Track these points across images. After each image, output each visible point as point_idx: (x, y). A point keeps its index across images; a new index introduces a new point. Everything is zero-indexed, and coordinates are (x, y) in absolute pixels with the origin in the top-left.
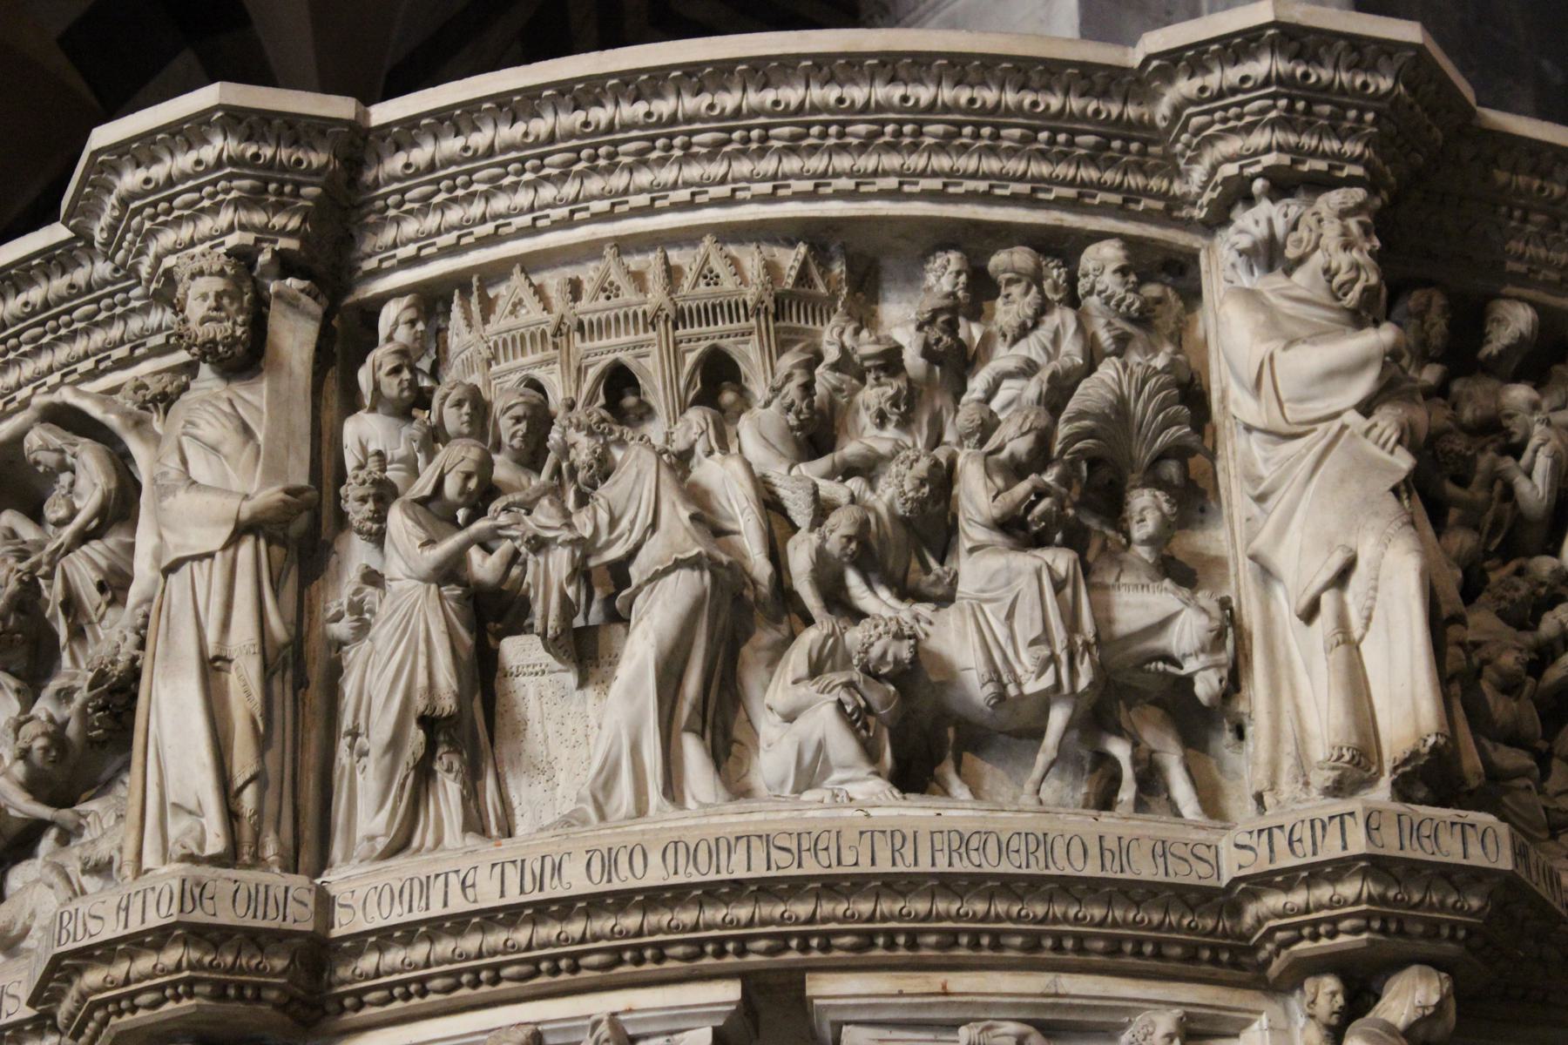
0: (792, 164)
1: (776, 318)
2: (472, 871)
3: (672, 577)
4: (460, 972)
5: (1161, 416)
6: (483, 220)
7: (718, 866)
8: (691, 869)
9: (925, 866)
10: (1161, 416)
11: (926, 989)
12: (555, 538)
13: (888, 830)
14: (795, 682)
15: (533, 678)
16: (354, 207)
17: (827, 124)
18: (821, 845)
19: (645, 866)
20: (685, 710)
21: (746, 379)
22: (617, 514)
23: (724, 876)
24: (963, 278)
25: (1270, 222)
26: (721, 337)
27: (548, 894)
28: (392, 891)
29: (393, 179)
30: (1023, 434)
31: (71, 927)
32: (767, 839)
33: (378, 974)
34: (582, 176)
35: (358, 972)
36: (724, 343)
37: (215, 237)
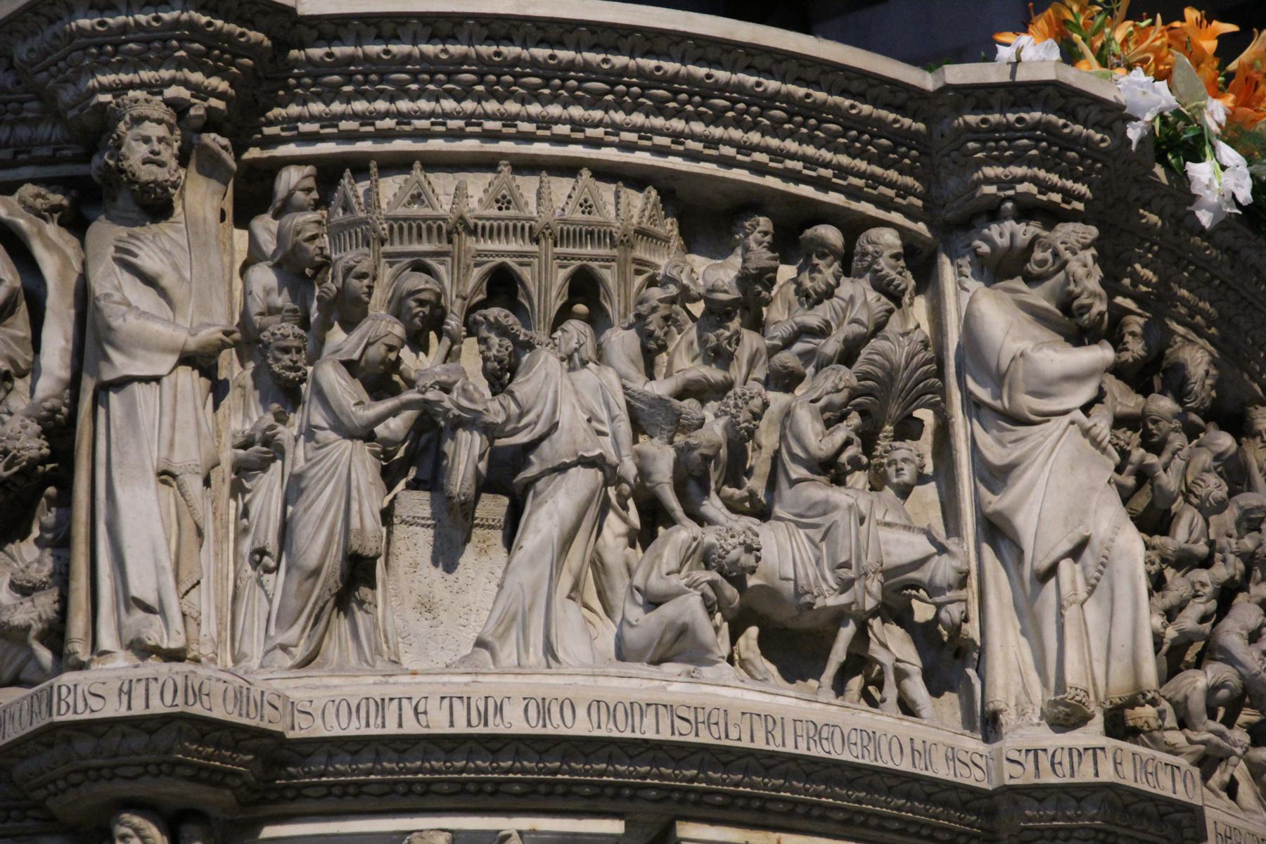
2: (423, 701)
7: (633, 727)
8: (611, 725)
9: (790, 748)
10: (921, 385)
18: (712, 721)
19: (574, 717)
23: (638, 735)
24: (768, 238)
25: (1012, 236)
26: (591, 260)
27: (491, 729)
30: (838, 391)
31: (70, 700)
32: (669, 707)
36: (594, 264)
37: (154, 88)
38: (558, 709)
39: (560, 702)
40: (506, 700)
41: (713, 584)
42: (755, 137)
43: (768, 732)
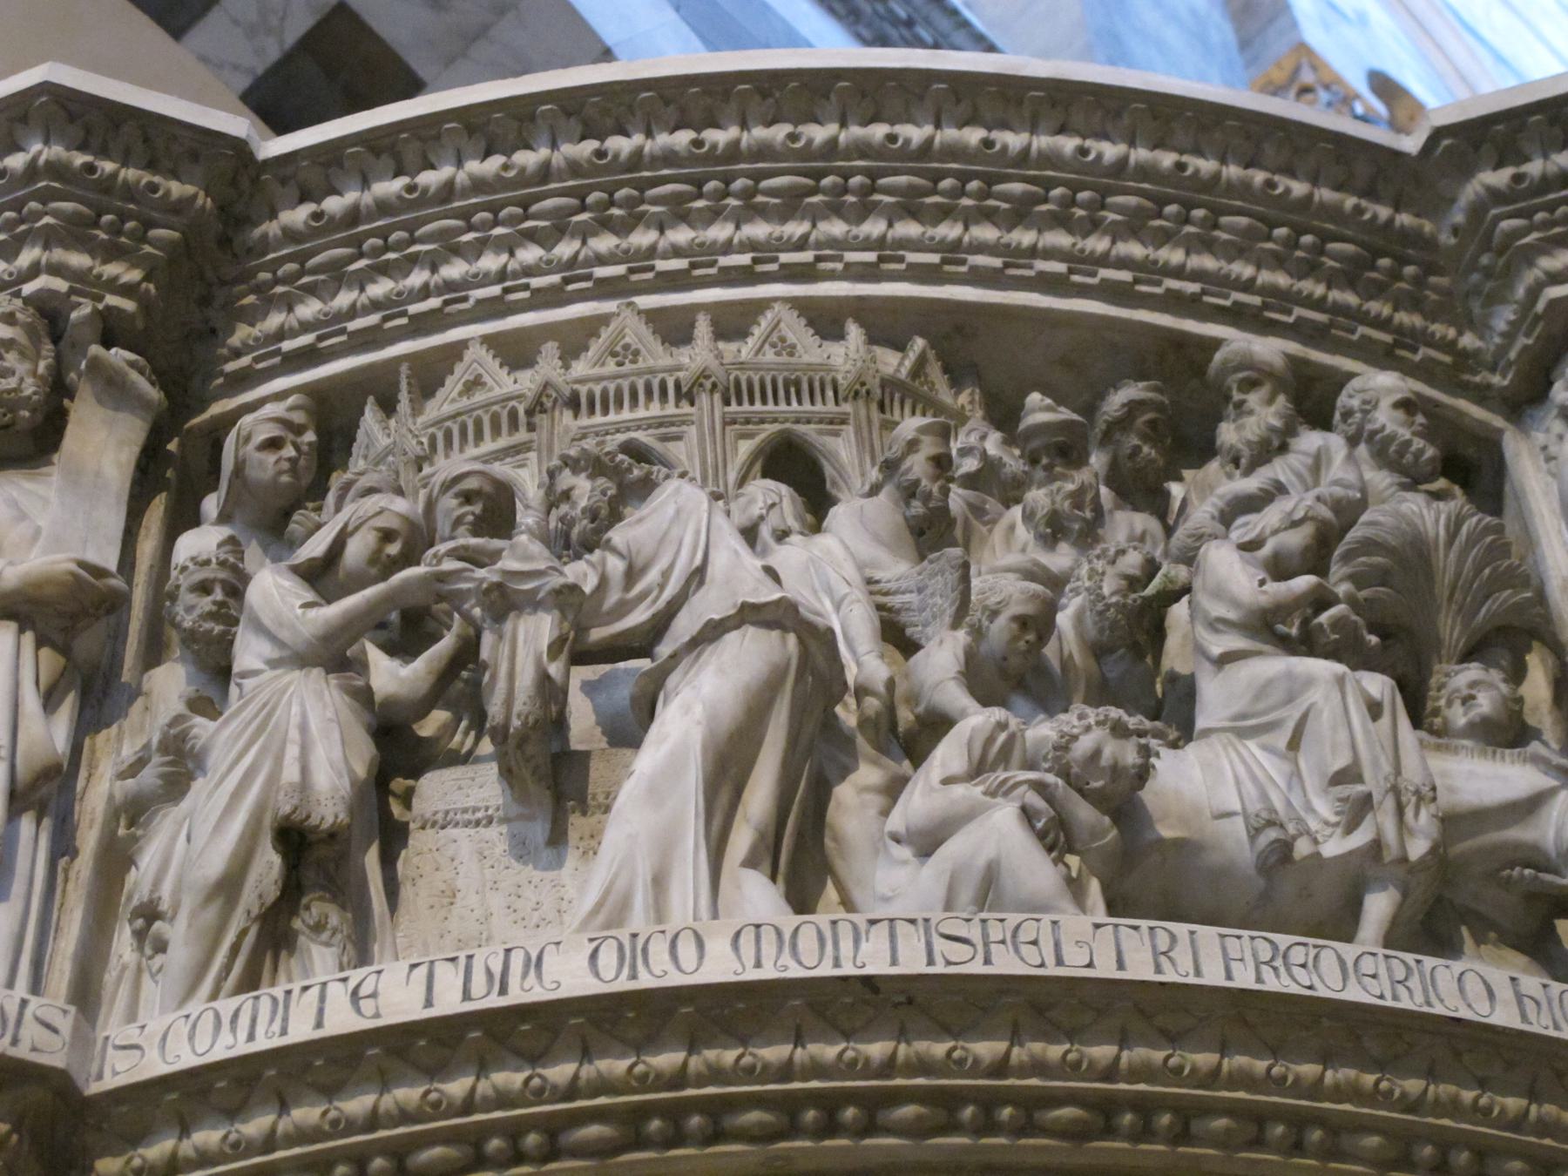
0: (909, 229)
1: (882, 408)
3: (732, 637)
5: (1487, 571)
6: (425, 292)
8: (786, 958)
10: (1487, 571)
12: (535, 591)
14: (947, 781)
15: (471, 831)
16: (223, 283)
17: (964, 177)
20: (742, 840)
21: (834, 483)
22: (639, 562)
23: (848, 969)
26: (797, 421)
29: (290, 235)
30: (1295, 524)
34: (585, 234)
36: (801, 428)
38: (666, 946)
39: (669, 936)
41: (1040, 787)
42: (1098, 244)
43: (1156, 953)
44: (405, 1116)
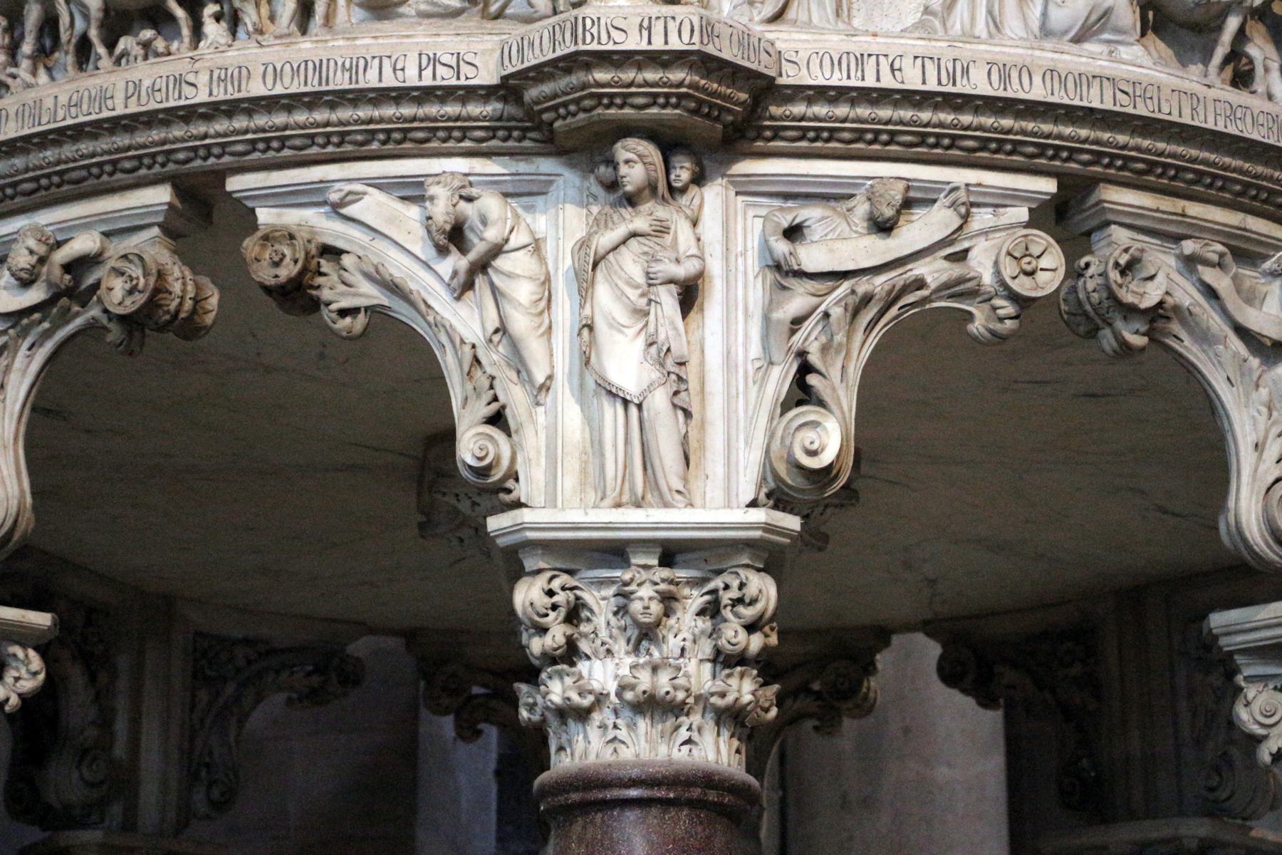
2: (898, 58)
4: (867, 131)
8: (1063, 93)
11: (1172, 210)
13: (1189, 92)
18: (1148, 95)
19: (1031, 84)
23: (1085, 104)
28: (831, 58)
31: (595, 31)
33: (802, 119)
35: (788, 113)
40: (971, 63)
43: (1193, 109)
44: (901, 122)
